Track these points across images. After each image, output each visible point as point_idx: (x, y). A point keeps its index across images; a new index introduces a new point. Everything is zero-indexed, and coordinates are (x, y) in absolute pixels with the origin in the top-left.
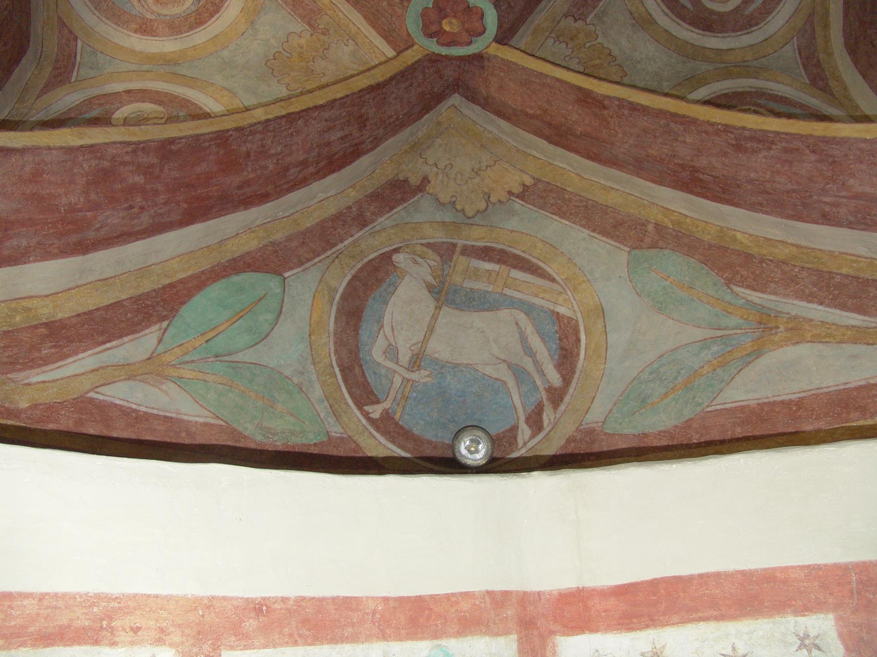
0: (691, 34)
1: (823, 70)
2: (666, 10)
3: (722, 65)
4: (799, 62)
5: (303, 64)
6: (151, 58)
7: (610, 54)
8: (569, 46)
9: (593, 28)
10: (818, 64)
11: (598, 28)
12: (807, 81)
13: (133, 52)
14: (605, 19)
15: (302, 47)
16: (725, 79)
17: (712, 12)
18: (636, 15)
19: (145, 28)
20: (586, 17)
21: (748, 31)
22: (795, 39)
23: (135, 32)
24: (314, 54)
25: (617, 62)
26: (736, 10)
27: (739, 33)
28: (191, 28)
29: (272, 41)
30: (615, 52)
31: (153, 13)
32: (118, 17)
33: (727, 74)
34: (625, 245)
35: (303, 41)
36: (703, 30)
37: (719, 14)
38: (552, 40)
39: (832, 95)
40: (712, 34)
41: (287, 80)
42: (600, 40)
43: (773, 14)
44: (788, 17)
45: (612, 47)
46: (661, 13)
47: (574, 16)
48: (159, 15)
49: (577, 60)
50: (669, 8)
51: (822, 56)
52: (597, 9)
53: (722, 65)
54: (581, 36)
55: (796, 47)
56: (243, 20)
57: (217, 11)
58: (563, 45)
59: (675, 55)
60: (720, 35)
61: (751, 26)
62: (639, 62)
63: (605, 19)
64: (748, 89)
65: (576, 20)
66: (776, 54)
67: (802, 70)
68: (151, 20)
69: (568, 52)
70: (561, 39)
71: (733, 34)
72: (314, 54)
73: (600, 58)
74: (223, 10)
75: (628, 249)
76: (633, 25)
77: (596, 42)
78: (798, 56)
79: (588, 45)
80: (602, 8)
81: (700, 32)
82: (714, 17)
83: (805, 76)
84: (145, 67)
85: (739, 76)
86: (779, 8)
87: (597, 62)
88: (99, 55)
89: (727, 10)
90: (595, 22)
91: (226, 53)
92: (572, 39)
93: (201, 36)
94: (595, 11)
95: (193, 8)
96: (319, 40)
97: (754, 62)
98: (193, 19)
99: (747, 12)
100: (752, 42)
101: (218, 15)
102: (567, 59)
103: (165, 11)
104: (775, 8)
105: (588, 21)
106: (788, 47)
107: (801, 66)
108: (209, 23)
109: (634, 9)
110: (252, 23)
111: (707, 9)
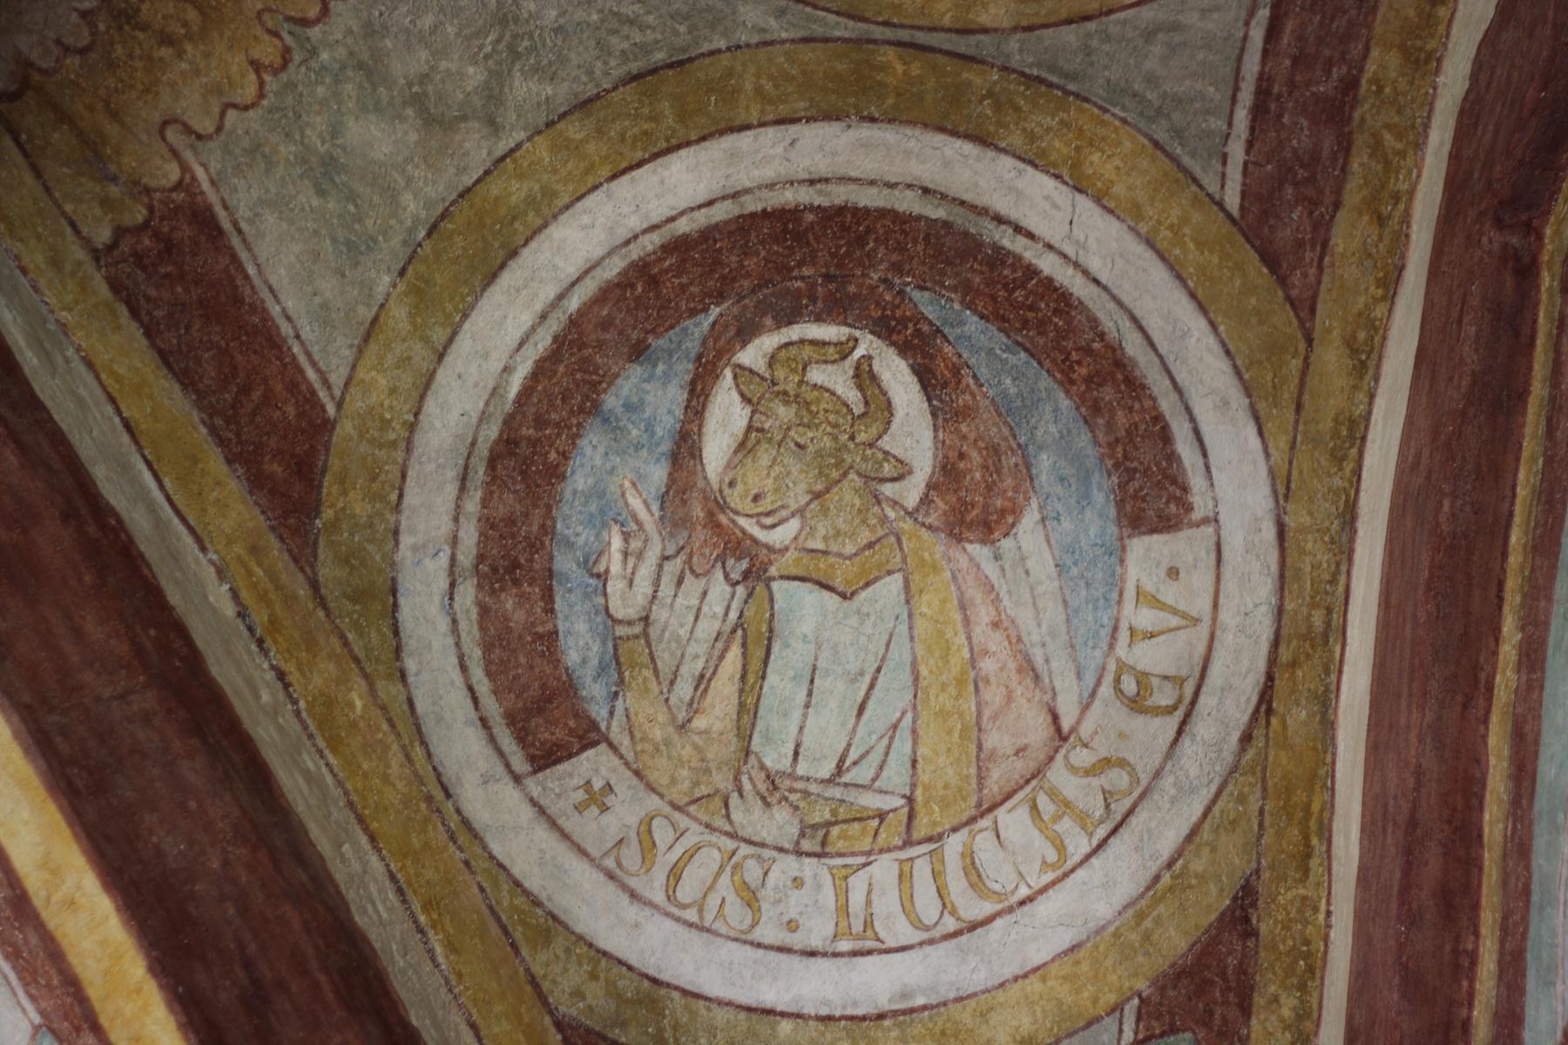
1: (1345, 147)
3: (845, 28)
4: (1252, 65)
10: (1337, 112)
12: (1232, 200)
16: (828, 117)
33: (848, 94)
34: (33, 998)
39: (1305, 308)
51: (1382, 62)
53: (845, 28)
64: (908, 203)
67: (1242, 116)
75: (37, 1020)
78: (1257, 34)
83: (1237, 151)
85: (905, 110)
97: (1013, 43)
107: (1246, 96)
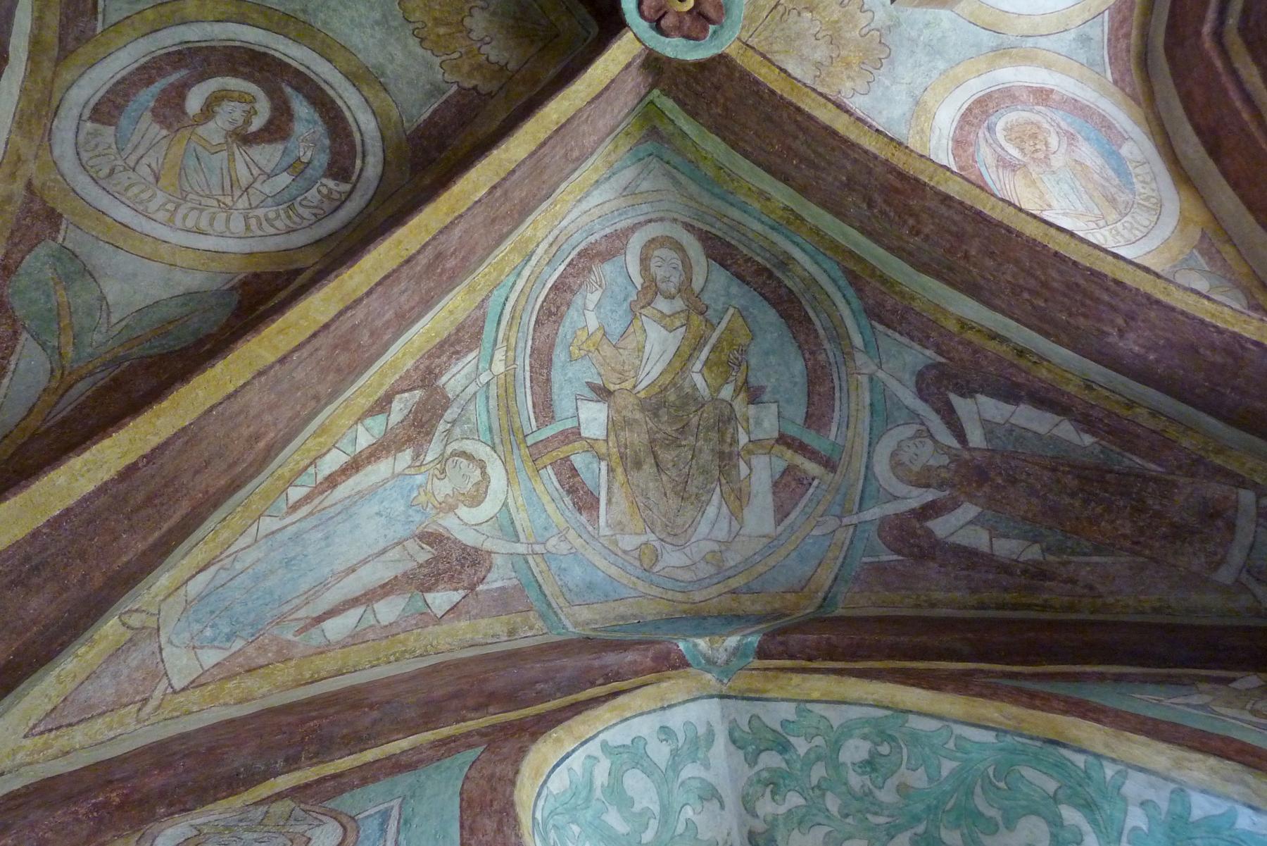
0: (287, 52)
2: (326, 87)
5: (843, 53)
6: (1028, 58)
7: (422, 40)
8: (484, 57)
9: (448, 77)
11: (440, 76)
13: (1048, 66)
14: (428, 87)
15: (849, 77)
17: (248, 77)
18: (378, 87)
19: (1042, 95)
20: (458, 92)
21: (185, 46)
22: (99, 30)
23: (1052, 91)
24: (832, 69)
25: (411, 27)
26: (202, 78)
27: (204, 44)
28: (989, 96)
29: (887, 83)
30: (413, 43)
31: (1039, 112)
32: (1076, 107)
35: (849, 84)
36: (265, 54)
37: (235, 73)
38: (509, 67)
40: (252, 47)
41: (863, 19)
42: (438, 60)
43: (136, 65)
44: (108, 60)
45: (420, 51)
46: (336, 86)
47: (478, 93)
48: (1031, 111)
49: (474, 36)
50: (321, 90)
52: (441, 101)
54: (466, 68)
55: (100, 17)
56: (930, 104)
57: (964, 116)
58: (492, 58)
59: (319, 25)
60: (237, 44)
61: (179, 52)
62: (377, 23)
63: (428, 87)
65: (475, 88)
66: (139, 7)
68: (1038, 104)
69: (485, 49)
70: (497, 67)
71: (213, 44)
72: (832, 69)
73: (438, 36)
74: (958, 118)
76: (383, 74)
77: (444, 58)
79: (456, 55)
80: (433, 100)
81: (272, 52)
82: (247, 70)
84: (1030, 43)
86: (124, 73)
87: (442, 31)
88: (1085, 61)
89: (220, 79)
90: (444, 85)
91: (941, 65)
92: (480, 66)
93: (975, 87)
94: (444, 97)
95: (993, 119)
96: (829, 87)
98: (991, 105)
99: (184, 72)
100: (182, 28)
101: (962, 111)
102: (487, 39)
103: (1026, 115)
104: (131, 74)
105: (455, 88)
106: (114, 18)
108: (969, 102)
109: (383, 95)
110: (917, 103)
111: (256, 82)
